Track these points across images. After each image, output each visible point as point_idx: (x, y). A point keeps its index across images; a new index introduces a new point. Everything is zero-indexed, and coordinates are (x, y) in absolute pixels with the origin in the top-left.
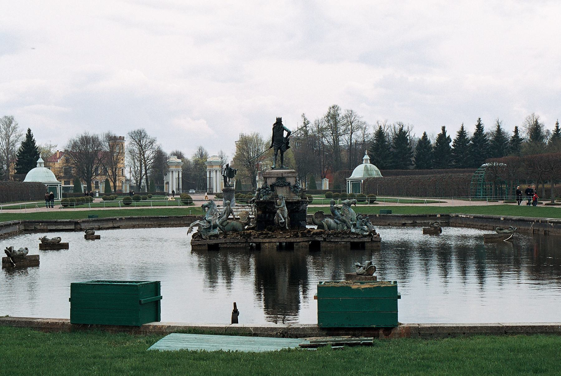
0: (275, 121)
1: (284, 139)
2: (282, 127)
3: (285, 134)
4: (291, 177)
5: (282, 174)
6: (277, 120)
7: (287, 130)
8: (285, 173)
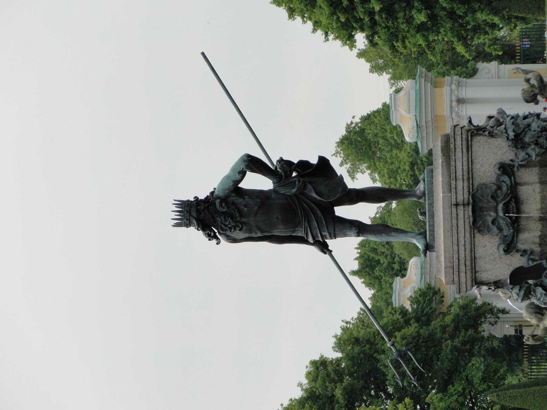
1: (282, 191)
2: (224, 200)
4: (471, 162)
6: (188, 226)
7: (238, 177)
8: (449, 188)
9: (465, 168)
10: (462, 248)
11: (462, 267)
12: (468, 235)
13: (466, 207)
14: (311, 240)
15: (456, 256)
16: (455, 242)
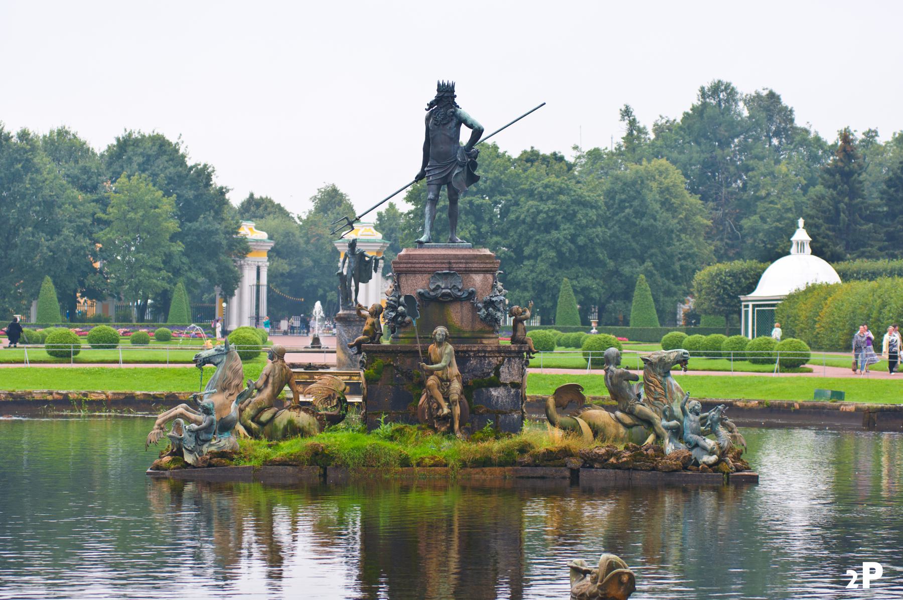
0: (432, 94)
2: (454, 114)
3: (465, 135)
6: (438, 90)
10: (422, 265)
12: (429, 269)
14: (426, 169)
15: (417, 261)
16: (426, 261)
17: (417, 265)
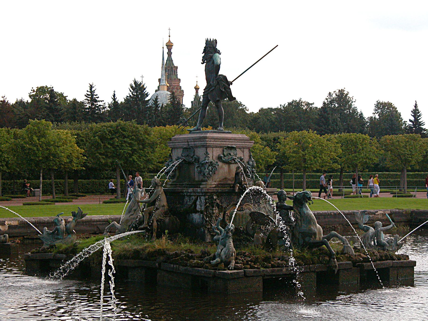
5: (188, 142)
9: (197, 145)
11: (173, 144)
13: (187, 145)
17: (177, 144)
